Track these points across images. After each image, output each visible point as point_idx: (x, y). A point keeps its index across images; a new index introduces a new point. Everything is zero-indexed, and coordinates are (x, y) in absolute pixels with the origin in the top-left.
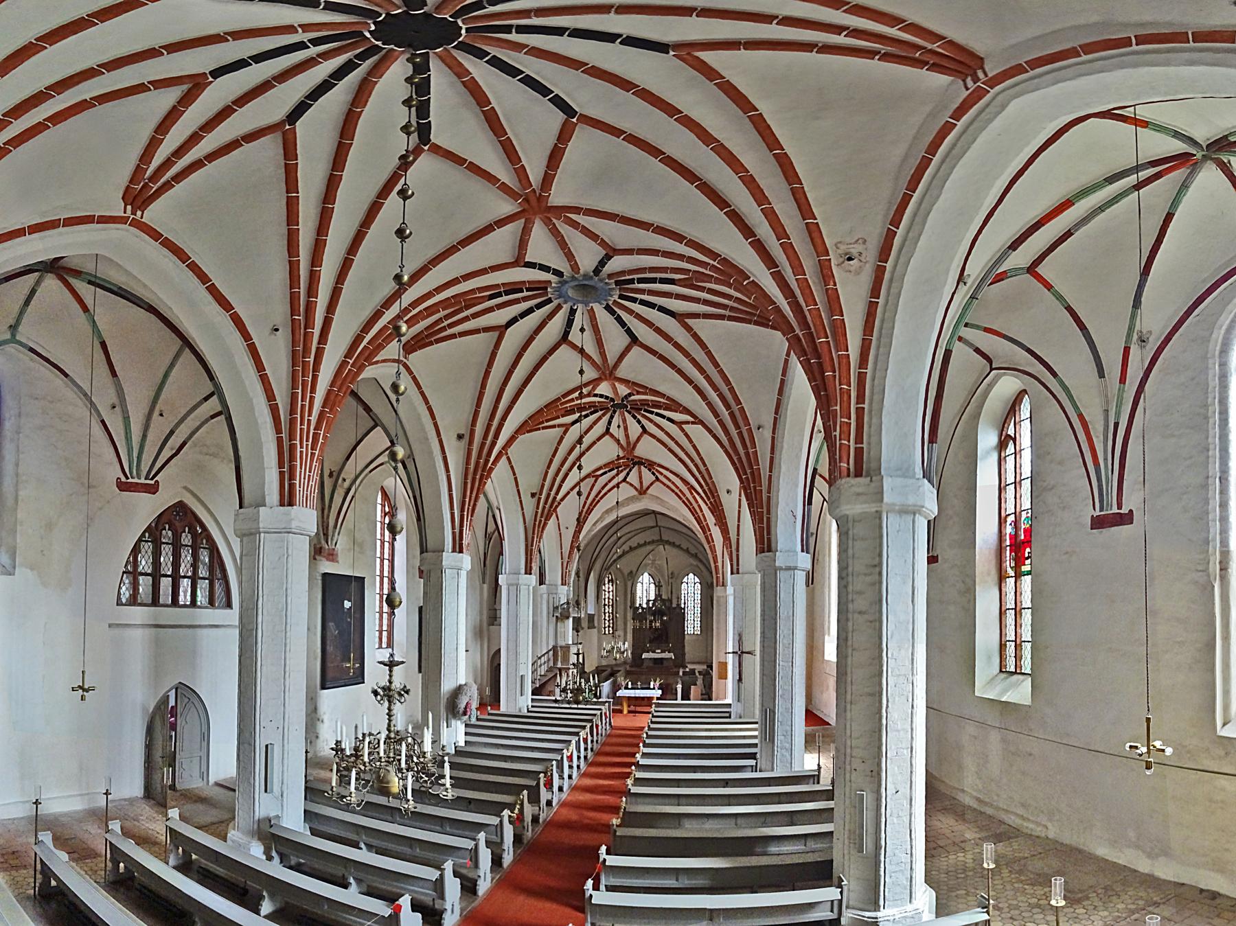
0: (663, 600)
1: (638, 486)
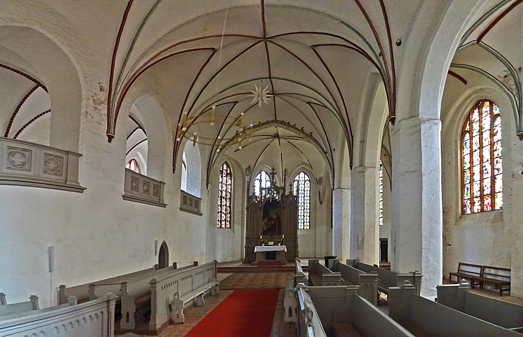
0: (277, 189)
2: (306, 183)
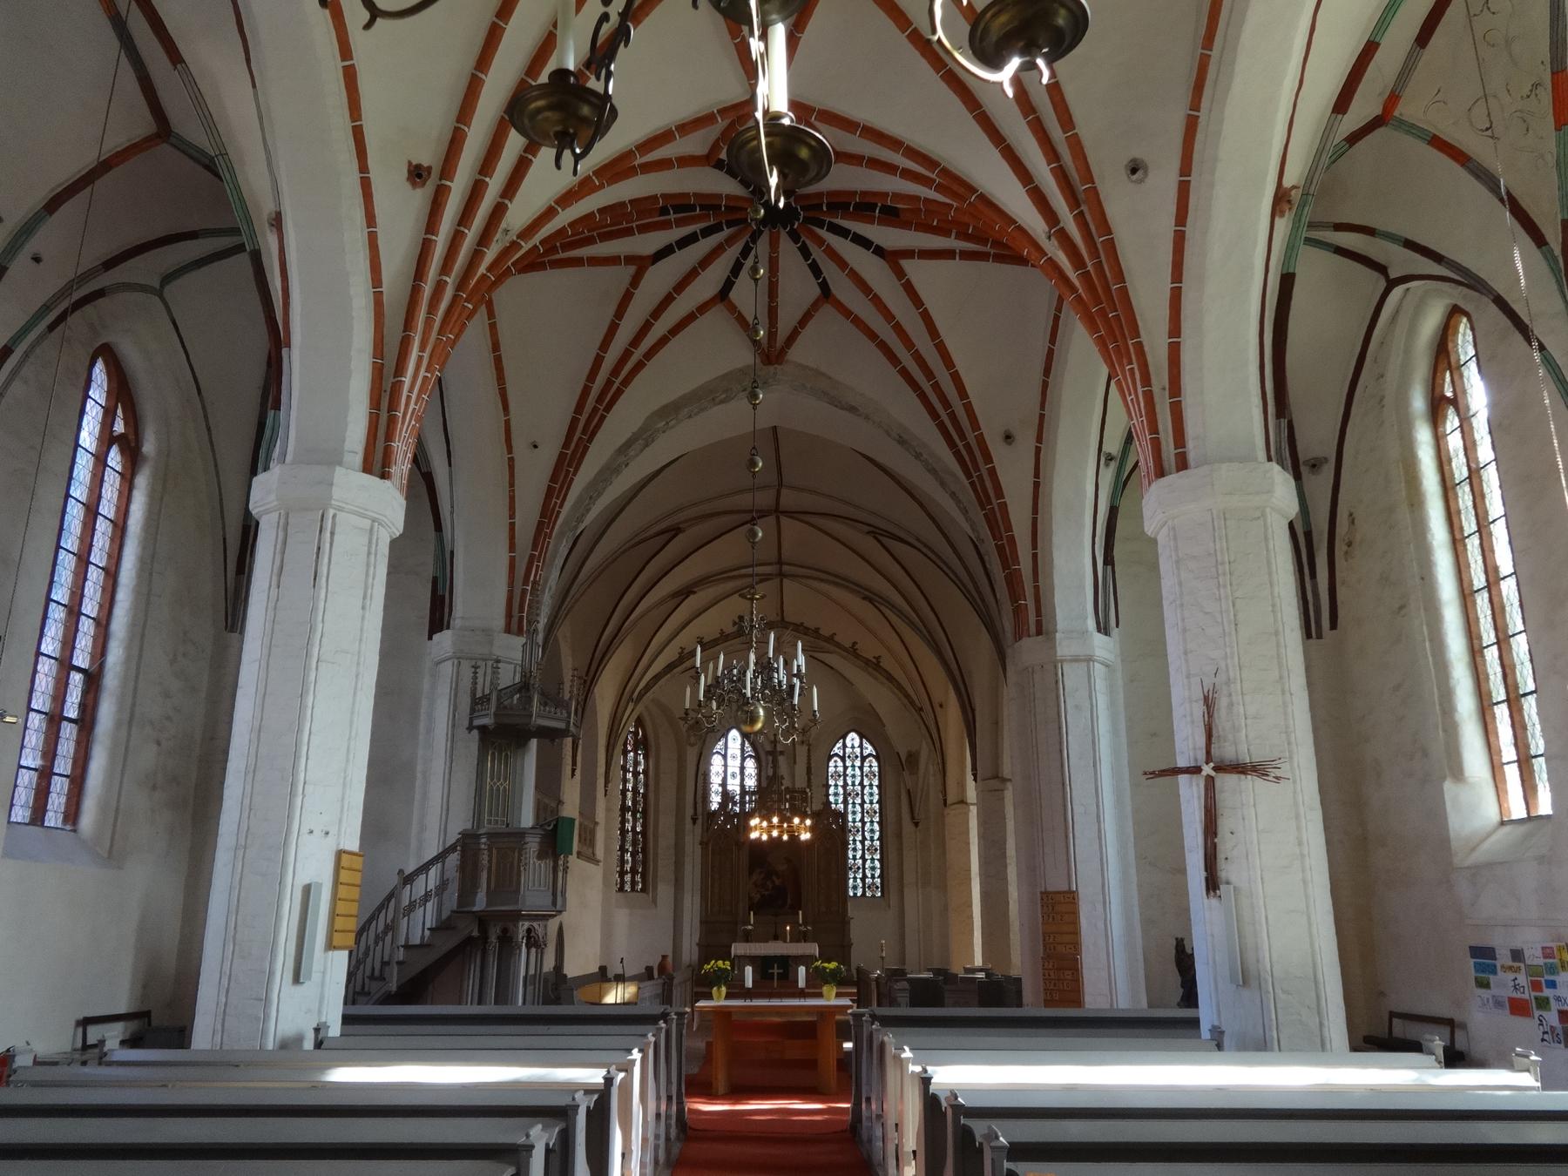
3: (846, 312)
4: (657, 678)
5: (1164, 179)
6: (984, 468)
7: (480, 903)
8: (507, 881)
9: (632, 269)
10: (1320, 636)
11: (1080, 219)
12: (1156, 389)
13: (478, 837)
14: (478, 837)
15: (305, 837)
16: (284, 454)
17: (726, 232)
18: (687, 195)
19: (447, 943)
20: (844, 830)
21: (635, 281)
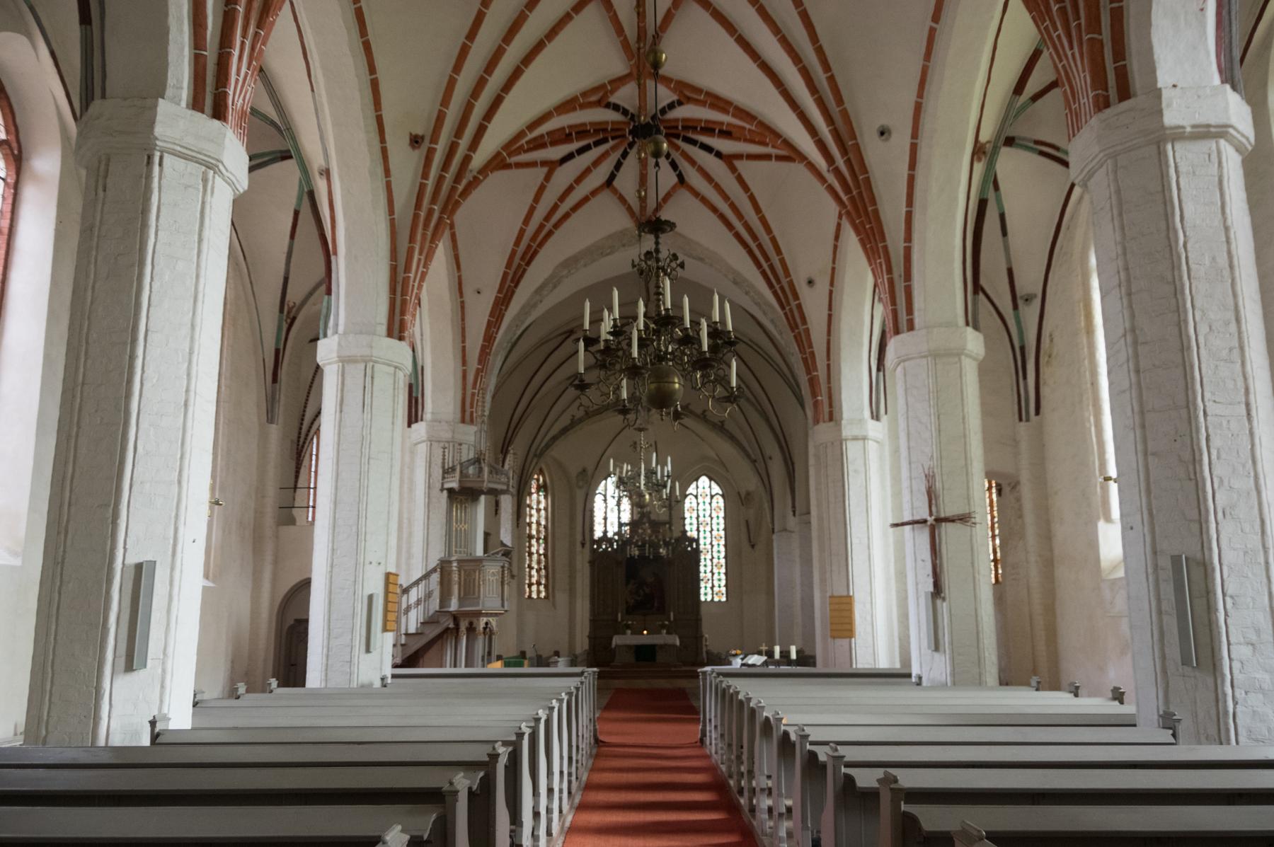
1: (635, 205)
2: (714, 500)
3: (696, 194)
4: (554, 439)
5: (901, 139)
6: (794, 304)
7: (454, 606)
8: (469, 591)
9: (545, 170)
10: (1028, 420)
11: (848, 163)
12: (896, 276)
13: (450, 562)
14: (450, 562)
15: (368, 567)
16: (336, 325)
17: (611, 143)
18: (585, 124)
19: (433, 632)
20: (697, 552)
21: (548, 178)
